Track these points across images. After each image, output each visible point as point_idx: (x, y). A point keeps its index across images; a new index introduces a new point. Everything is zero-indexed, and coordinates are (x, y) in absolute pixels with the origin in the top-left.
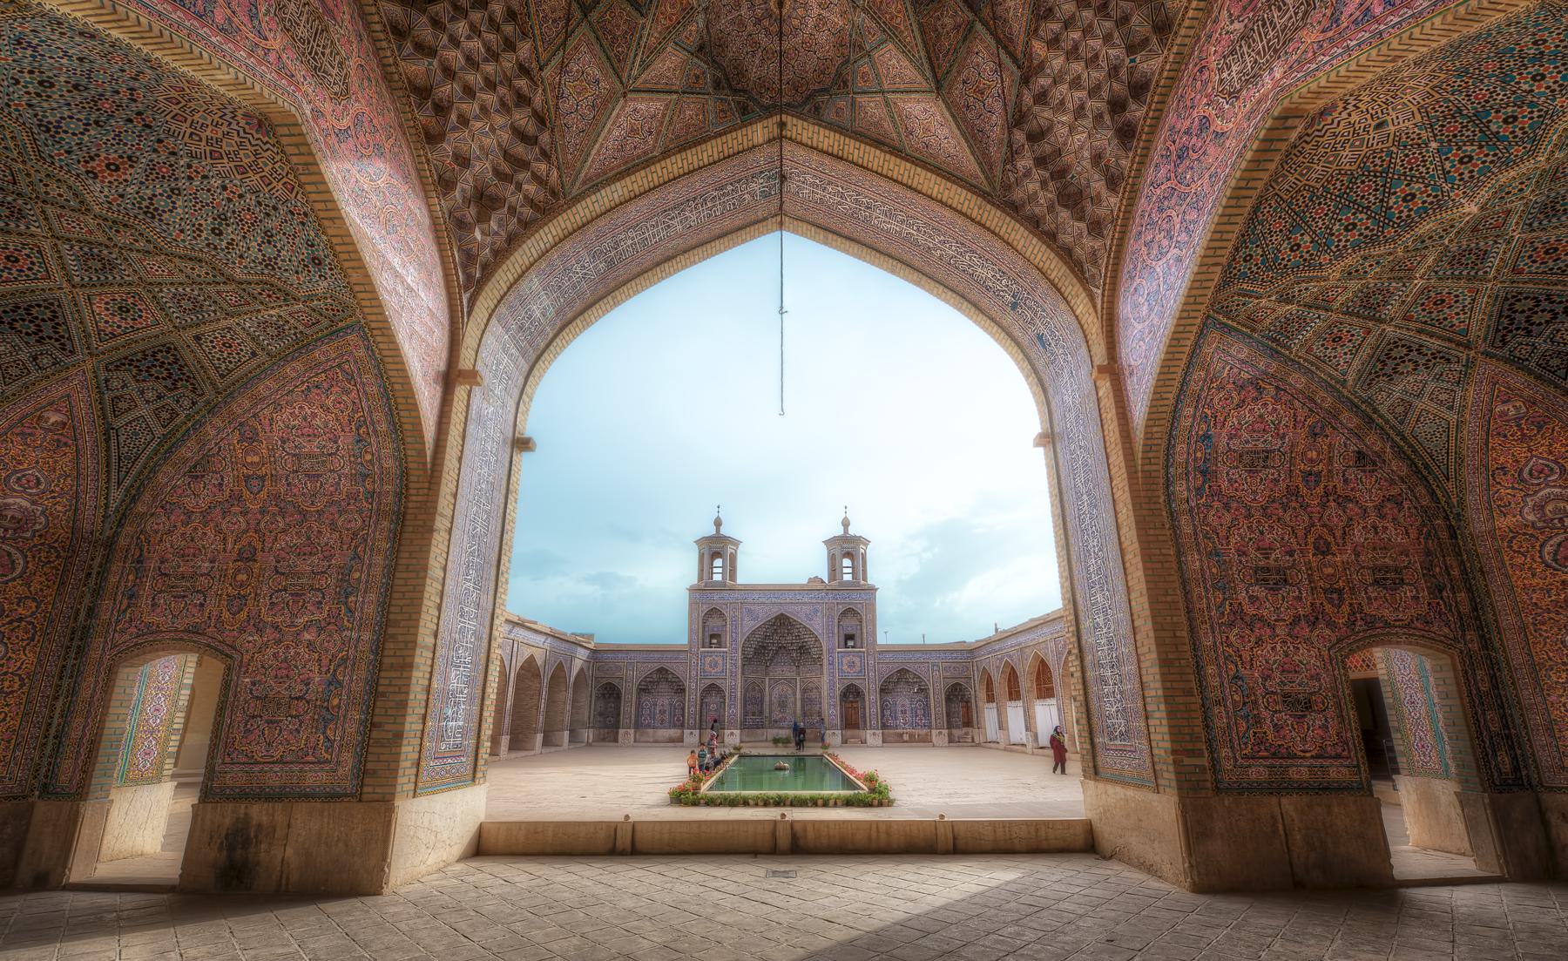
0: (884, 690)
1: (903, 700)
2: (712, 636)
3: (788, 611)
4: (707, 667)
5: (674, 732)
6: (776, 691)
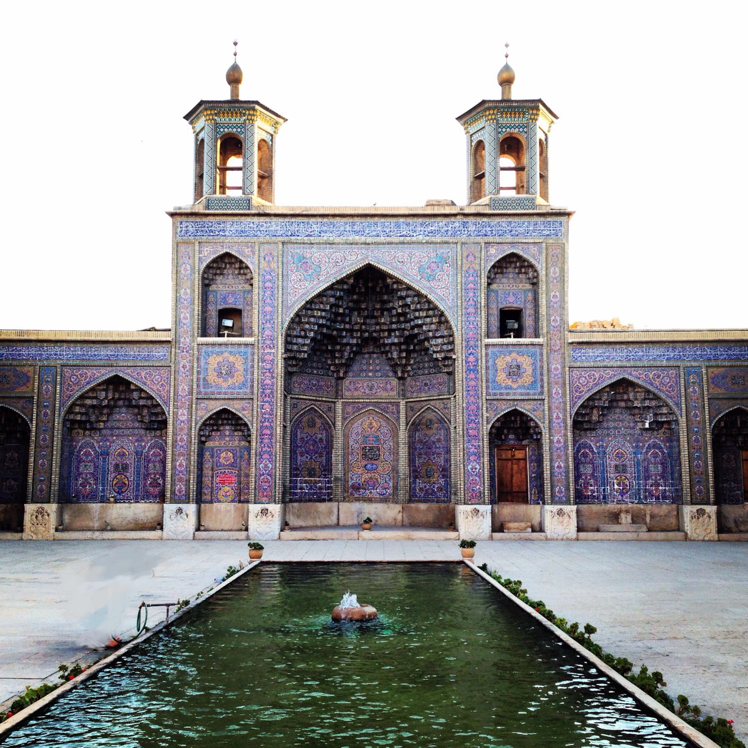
0: (582, 424)
1: (620, 444)
2: (225, 313)
3: (387, 261)
4: (212, 377)
5: (144, 510)
6: (357, 427)
